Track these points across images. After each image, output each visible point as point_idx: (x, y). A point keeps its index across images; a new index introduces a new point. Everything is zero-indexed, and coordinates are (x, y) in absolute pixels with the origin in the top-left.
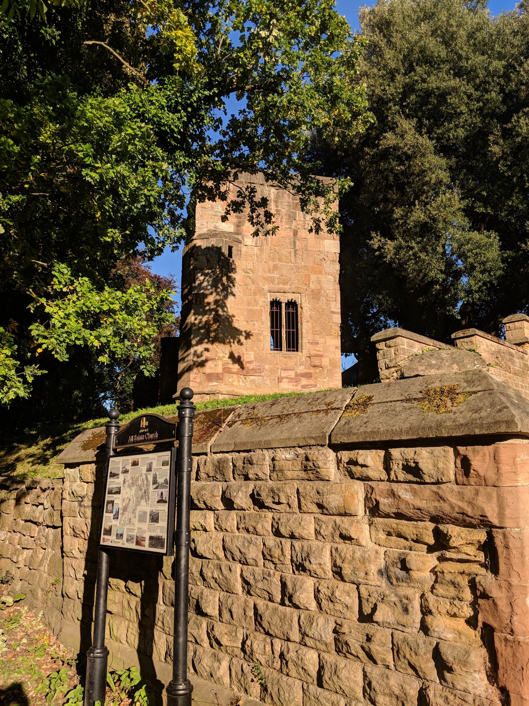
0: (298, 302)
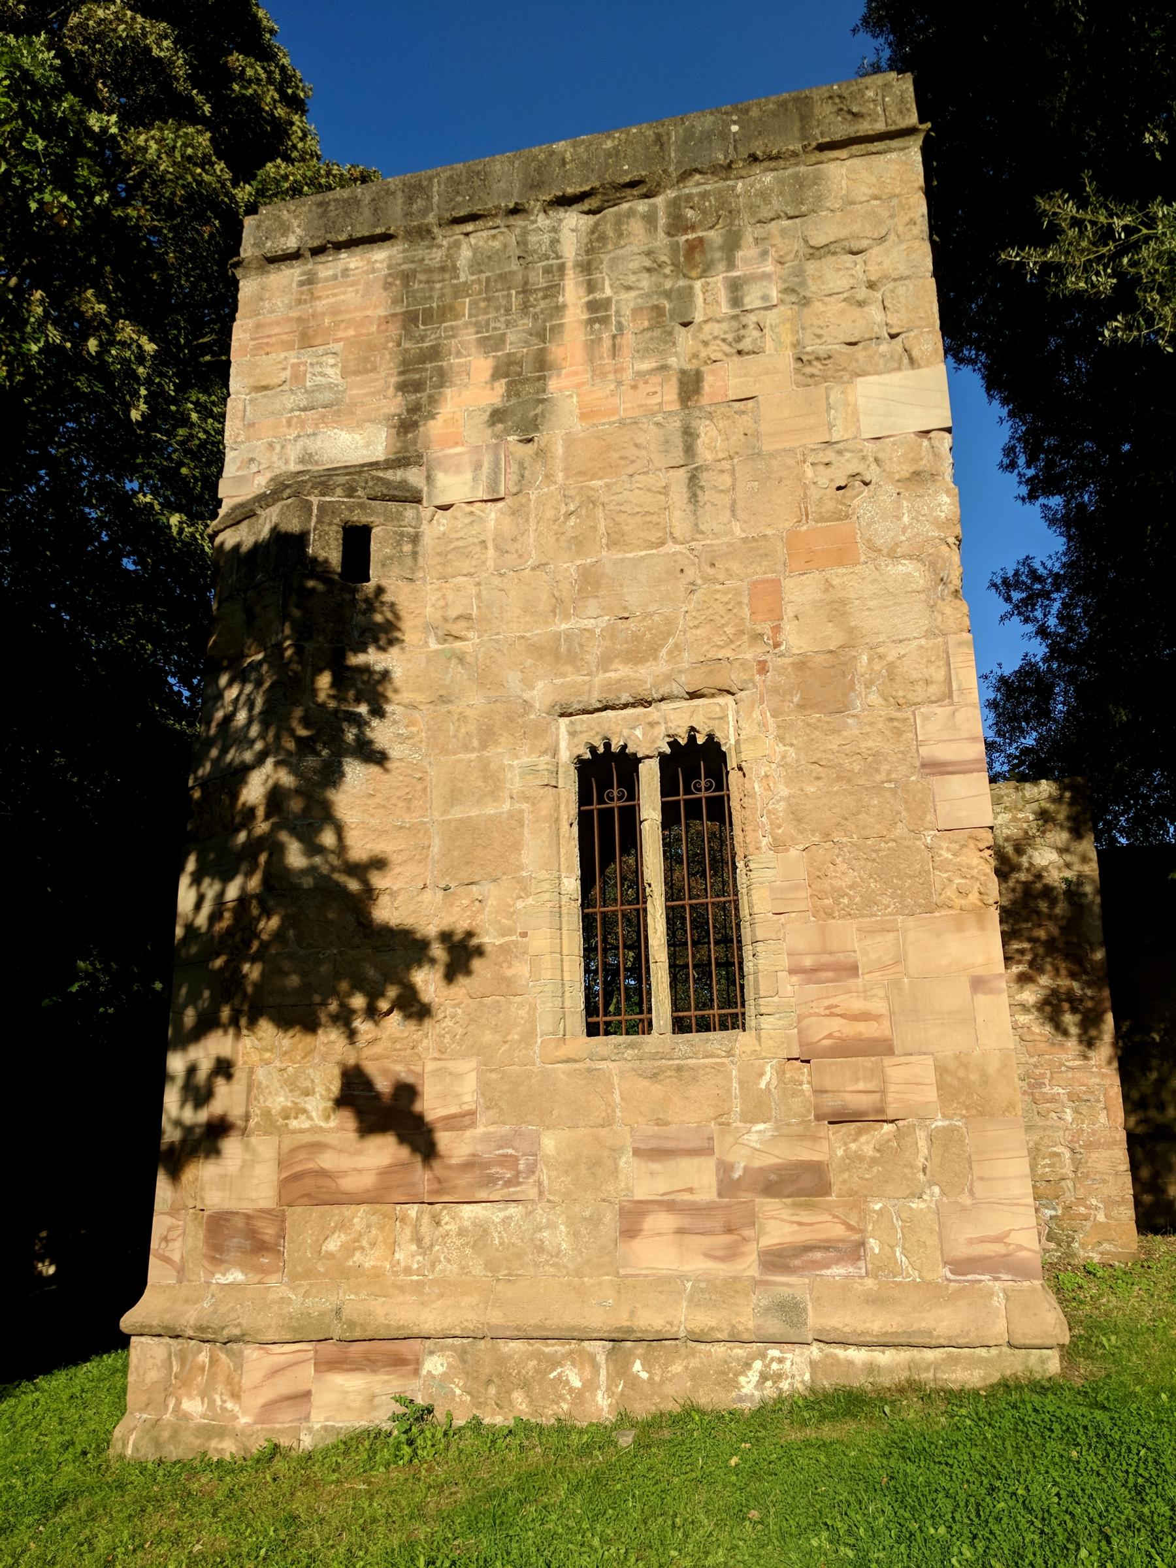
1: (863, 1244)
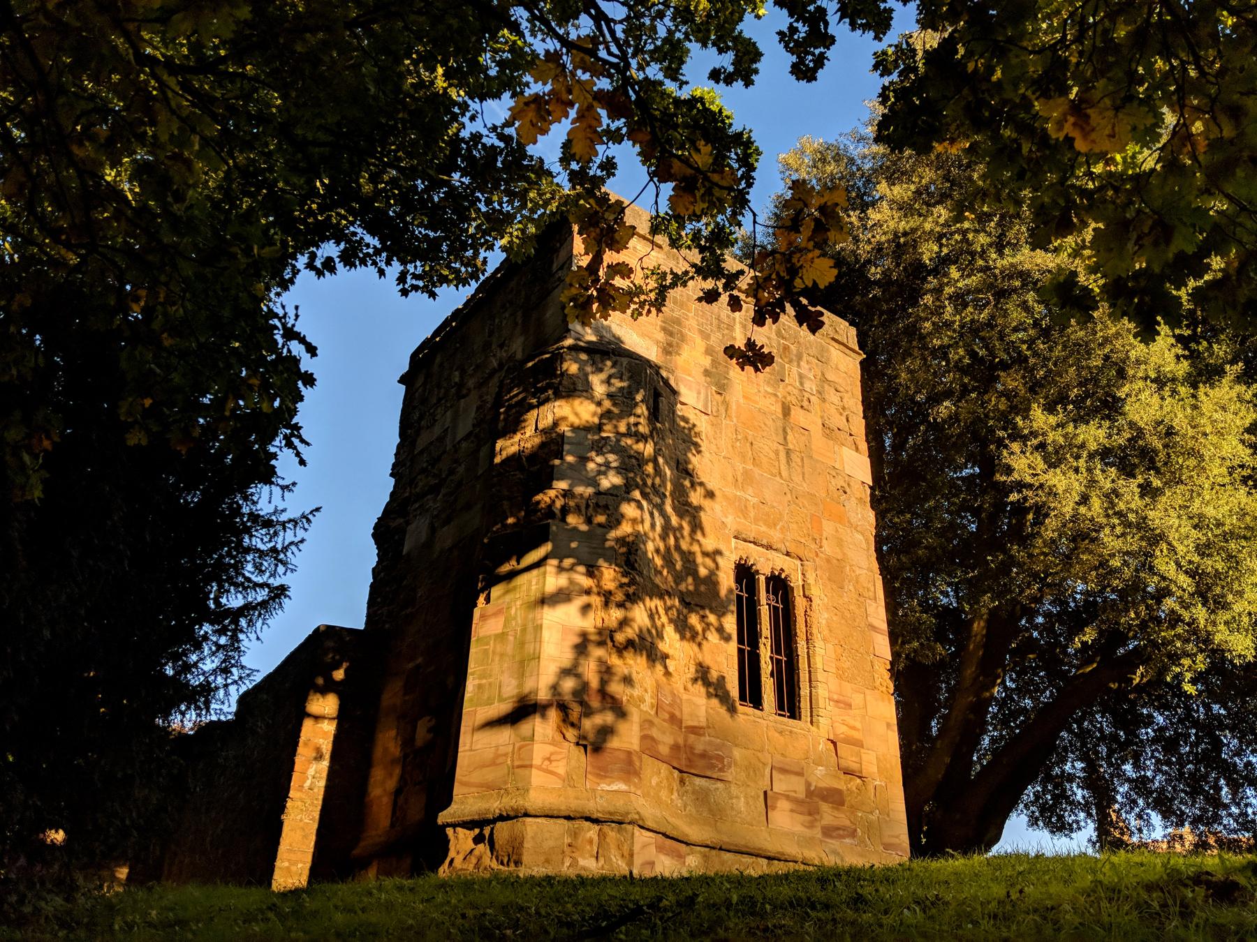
0: (796, 582)
1: (856, 830)
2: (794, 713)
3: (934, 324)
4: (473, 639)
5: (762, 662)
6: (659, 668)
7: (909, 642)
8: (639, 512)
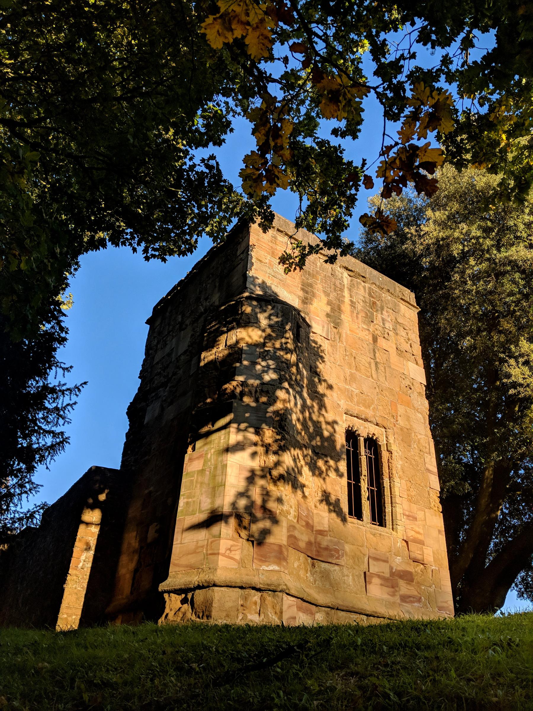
0: (382, 442)
1: (421, 598)
2: (382, 523)
3: (460, 291)
4: (184, 474)
5: (363, 491)
6: (299, 493)
7: (449, 481)
8: (287, 395)
